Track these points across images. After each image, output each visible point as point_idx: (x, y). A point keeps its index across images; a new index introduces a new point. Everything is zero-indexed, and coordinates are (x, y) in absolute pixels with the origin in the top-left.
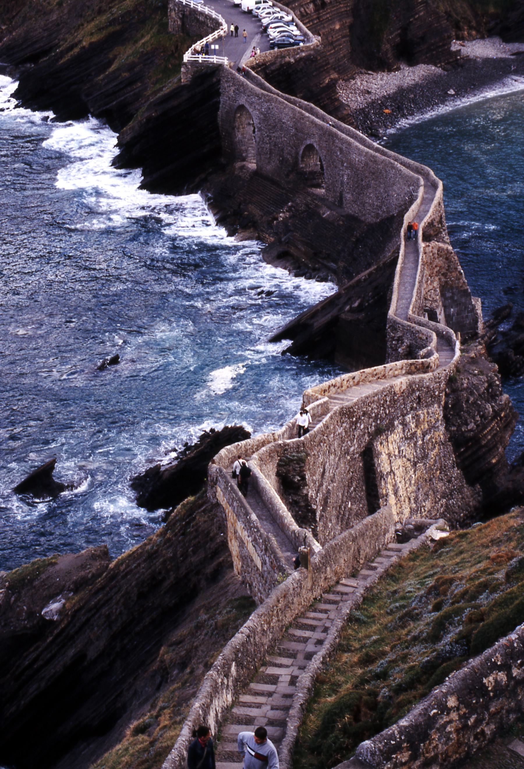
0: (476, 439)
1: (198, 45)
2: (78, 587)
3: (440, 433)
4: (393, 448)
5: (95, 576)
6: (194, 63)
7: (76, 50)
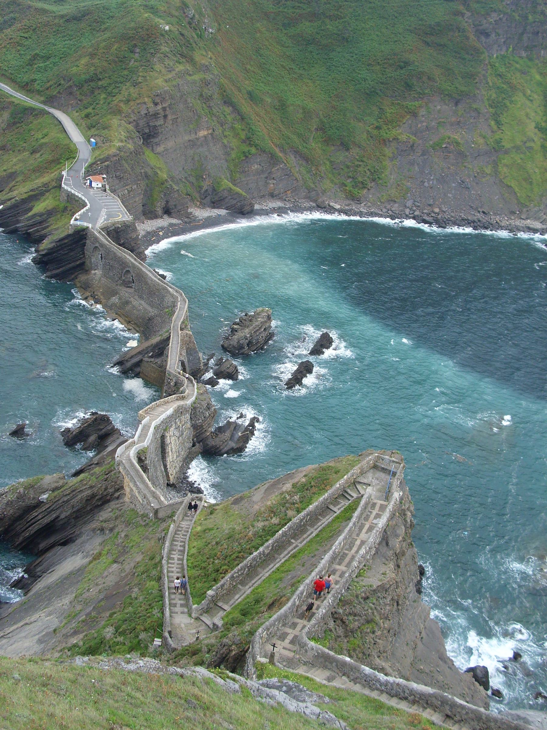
0: (201, 426)
1: (77, 216)
2: (53, 490)
3: (189, 425)
4: (171, 433)
5: (61, 487)
6: (76, 226)
7: (13, 200)
